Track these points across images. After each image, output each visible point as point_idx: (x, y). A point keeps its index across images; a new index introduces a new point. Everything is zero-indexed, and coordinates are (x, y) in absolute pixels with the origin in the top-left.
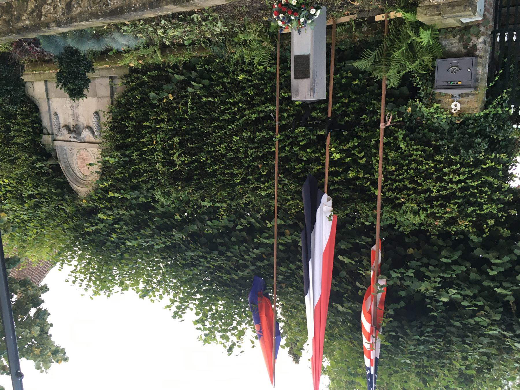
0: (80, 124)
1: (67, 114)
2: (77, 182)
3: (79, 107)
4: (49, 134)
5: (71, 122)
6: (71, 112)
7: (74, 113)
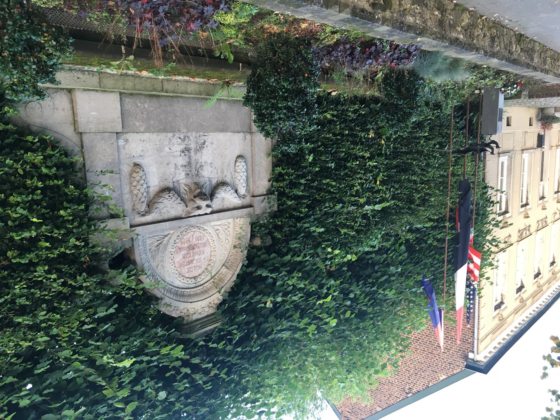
0: (202, 181)
1: (172, 166)
2: (183, 295)
3: (204, 151)
4: (113, 216)
5: (181, 178)
6: (182, 161)
7: (189, 163)
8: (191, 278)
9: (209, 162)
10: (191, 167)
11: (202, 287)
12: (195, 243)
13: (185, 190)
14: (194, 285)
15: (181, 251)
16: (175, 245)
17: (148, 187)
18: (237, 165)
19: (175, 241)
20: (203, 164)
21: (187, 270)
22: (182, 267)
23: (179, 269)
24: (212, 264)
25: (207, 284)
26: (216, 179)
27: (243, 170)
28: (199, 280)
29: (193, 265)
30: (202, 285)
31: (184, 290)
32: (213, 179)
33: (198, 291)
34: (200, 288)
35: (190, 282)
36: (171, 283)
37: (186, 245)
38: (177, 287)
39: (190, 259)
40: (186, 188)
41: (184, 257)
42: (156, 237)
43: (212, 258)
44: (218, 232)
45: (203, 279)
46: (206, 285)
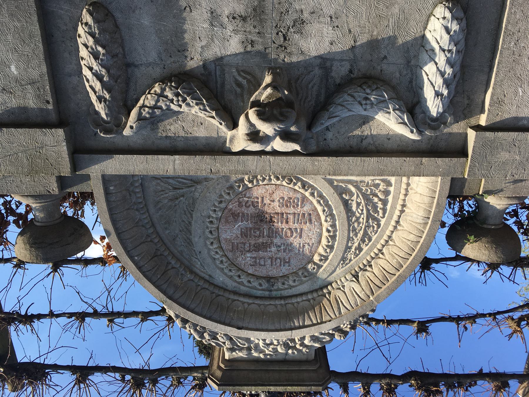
9: (329, 10)
10: (261, 21)
11: (282, 302)
12: (279, 210)
13: (239, 85)
14: (267, 293)
15: (236, 221)
16: (223, 205)
17: (128, 65)
20: (306, 15)
22: (238, 254)
23: (230, 255)
25: (299, 299)
26: (347, 66)
29: (270, 254)
31: (236, 298)
32: (335, 63)
33: (271, 309)
34: (278, 302)
35: (256, 284)
36: (207, 277)
37: (251, 210)
38: (220, 288)
39: (261, 240)
40: (240, 79)
41: (245, 234)
42: (171, 181)
45: (291, 287)
46: (294, 300)
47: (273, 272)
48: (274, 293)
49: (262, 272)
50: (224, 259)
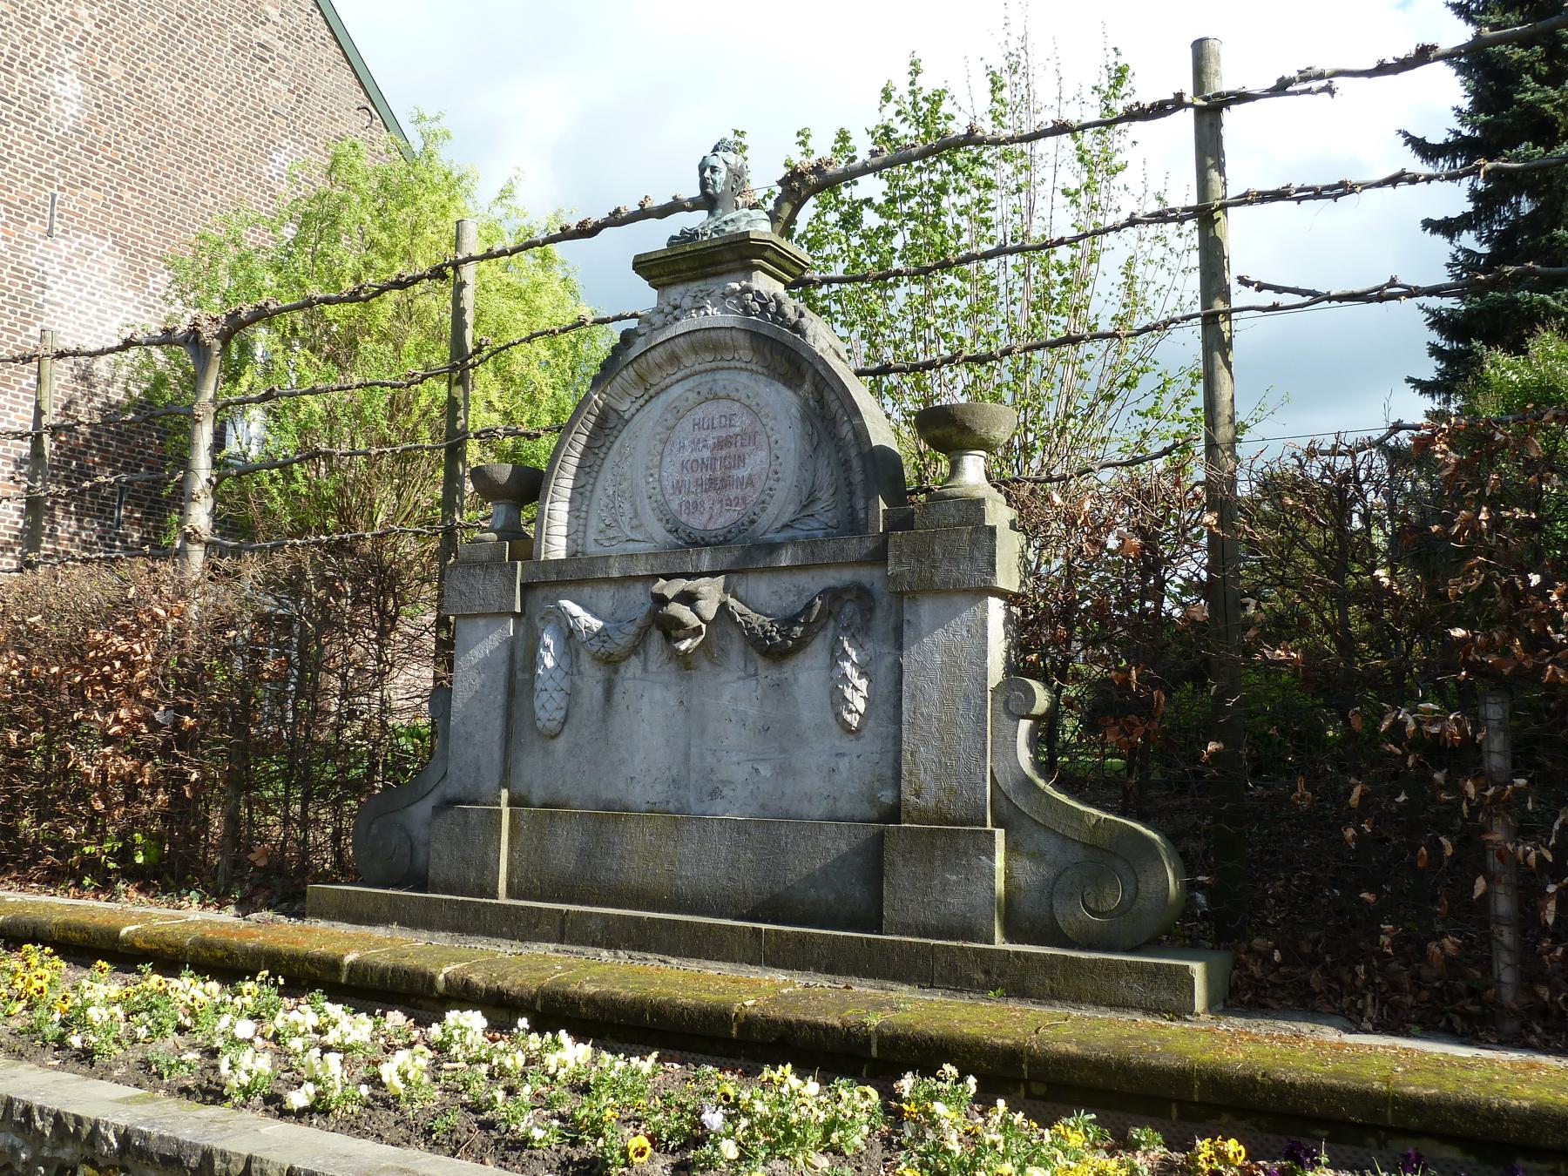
8: (728, 397)
11: (697, 368)
18: (563, 712)
19: (763, 509)
21: (737, 421)
23: (759, 427)
24: (659, 429)
27: (544, 696)
28: (704, 391)
29: (715, 434)
30: (696, 373)
34: (702, 367)
37: (734, 493)
41: (741, 459)
43: (659, 447)
44: (635, 522)
47: (712, 410)
48: (709, 377)
49: (724, 407)
50: (765, 421)
